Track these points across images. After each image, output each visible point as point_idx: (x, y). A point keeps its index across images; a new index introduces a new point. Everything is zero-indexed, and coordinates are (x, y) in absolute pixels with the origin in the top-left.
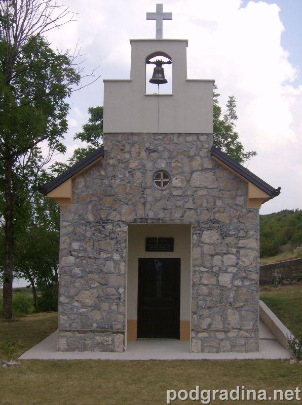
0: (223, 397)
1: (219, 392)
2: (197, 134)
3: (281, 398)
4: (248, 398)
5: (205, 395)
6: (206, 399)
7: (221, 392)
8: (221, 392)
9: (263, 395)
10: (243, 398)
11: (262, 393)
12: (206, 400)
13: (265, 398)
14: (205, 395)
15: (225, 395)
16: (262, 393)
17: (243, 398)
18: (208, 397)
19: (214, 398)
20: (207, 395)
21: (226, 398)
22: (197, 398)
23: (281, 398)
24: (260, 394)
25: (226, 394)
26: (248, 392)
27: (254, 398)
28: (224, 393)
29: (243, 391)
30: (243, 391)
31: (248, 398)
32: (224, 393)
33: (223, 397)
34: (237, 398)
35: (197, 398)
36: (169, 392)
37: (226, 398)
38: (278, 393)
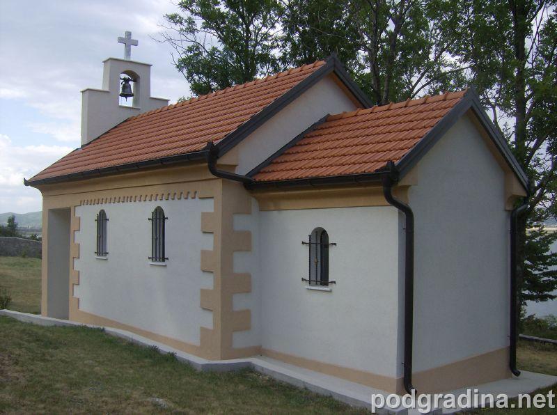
0: (448, 404)
1: (443, 397)
3: (529, 406)
5: (424, 400)
6: (425, 406)
7: (446, 397)
8: (446, 397)
12: (426, 408)
18: (428, 404)
19: (436, 406)
21: (453, 405)
23: (529, 406)
25: (453, 400)
26: (483, 397)
28: (449, 398)
29: (476, 396)
30: (476, 396)
32: (449, 398)
33: (448, 404)
34: (468, 405)
37: (453, 405)
38: (525, 399)
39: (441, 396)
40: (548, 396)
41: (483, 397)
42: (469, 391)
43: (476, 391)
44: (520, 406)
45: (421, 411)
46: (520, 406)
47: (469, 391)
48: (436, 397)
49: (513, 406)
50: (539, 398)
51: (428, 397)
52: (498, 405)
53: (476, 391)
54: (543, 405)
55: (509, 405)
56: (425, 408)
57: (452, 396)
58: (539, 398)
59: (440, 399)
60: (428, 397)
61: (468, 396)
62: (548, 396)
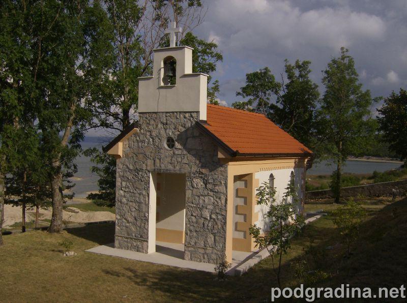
0: (328, 295)
1: (324, 290)
2: (191, 112)
3: (386, 296)
4: (353, 296)
5: (310, 293)
6: (310, 297)
7: (326, 290)
8: (326, 290)
9: (368, 293)
10: (348, 296)
11: (367, 291)
12: (311, 298)
13: (370, 296)
14: (310, 293)
15: (329, 293)
16: (367, 291)
17: (348, 296)
18: (313, 295)
19: (319, 296)
20: (312, 294)
21: (331, 296)
22: (302, 296)
23: (386, 296)
24: (364, 292)
25: (331, 292)
26: (353, 290)
27: (359, 296)
28: (328, 291)
29: (348, 290)
30: (348, 290)
31: (353, 296)
32: (328, 291)
33: (328, 295)
34: (342, 296)
35: (302, 296)
36: (273, 290)
37: (331, 296)
38: (383, 292)
39: (322, 289)
40: (400, 289)
41: (353, 290)
42: (343, 286)
43: (348, 285)
44: (380, 296)
45: (307, 300)
46: (380, 296)
47: (343, 286)
48: (319, 290)
49: (375, 296)
50: (394, 291)
51: (313, 290)
52: (364, 296)
53: (348, 285)
54: (397, 296)
55: (372, 296)
56: (311, 298)
57: (331, 289)
58: (394, 291)
59: (321, 291)
60: (313, 290)
61: (342, 290)
62: (400, 289)
